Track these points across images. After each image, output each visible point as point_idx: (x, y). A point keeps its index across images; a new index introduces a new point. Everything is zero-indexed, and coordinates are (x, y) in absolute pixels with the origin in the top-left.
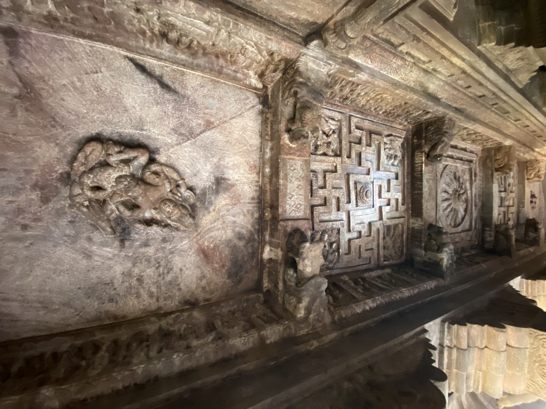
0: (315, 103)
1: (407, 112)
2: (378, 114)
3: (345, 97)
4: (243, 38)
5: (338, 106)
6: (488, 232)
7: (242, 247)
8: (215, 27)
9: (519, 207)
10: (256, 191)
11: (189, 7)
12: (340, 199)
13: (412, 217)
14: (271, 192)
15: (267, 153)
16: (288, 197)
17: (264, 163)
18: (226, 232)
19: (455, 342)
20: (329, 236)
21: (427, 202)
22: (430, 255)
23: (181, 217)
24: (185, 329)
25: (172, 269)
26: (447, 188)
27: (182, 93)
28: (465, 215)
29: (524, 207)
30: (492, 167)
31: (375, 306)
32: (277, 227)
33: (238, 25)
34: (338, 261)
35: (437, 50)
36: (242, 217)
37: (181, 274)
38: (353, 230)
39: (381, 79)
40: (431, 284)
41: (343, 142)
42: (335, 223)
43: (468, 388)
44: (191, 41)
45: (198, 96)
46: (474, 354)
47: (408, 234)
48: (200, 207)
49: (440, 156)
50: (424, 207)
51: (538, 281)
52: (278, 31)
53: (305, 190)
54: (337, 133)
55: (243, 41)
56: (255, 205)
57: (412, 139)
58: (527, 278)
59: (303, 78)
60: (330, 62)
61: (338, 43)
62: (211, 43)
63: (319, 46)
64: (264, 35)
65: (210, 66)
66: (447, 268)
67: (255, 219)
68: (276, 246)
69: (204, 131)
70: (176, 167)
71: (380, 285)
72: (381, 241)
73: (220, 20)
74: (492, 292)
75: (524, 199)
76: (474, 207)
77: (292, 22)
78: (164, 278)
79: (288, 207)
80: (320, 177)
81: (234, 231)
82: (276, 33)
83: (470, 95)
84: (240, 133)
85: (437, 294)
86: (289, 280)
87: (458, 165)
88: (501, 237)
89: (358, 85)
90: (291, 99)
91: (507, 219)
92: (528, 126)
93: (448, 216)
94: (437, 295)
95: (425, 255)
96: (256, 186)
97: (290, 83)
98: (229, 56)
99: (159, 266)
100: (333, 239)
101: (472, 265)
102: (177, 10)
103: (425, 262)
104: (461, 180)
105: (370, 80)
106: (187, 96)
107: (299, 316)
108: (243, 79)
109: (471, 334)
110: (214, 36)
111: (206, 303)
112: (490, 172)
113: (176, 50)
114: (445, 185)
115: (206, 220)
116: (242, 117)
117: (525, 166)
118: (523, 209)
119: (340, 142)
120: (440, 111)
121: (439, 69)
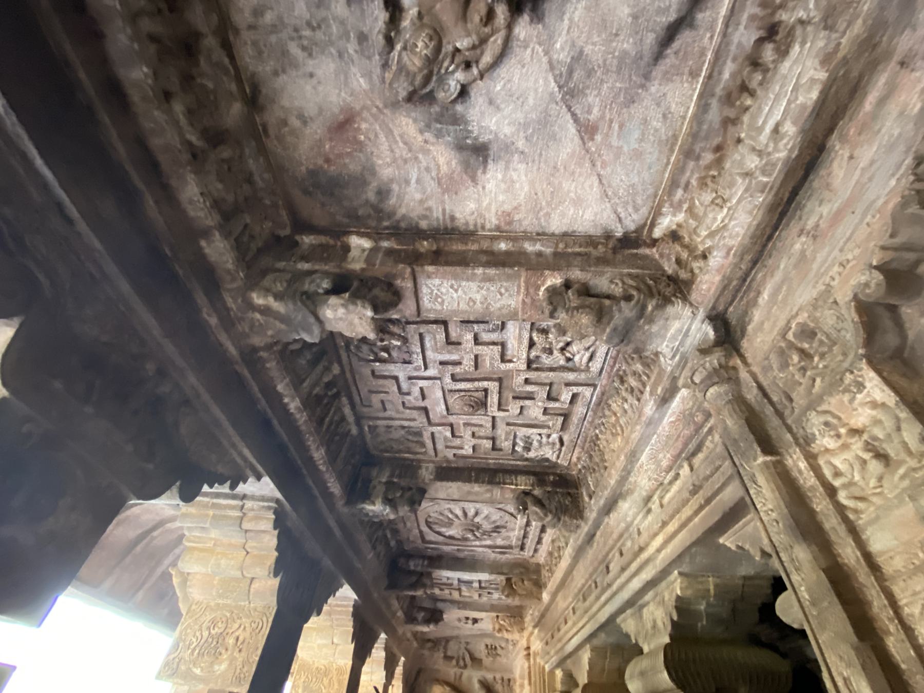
0: (608, 330)
1: (594, 470)
2: (596, 428)
3: (625, 378)
4: (739, 202)
5: (612, 367)
7: (364, 197)
8: (767, 145)
10: (467, 224)
11: (809, 90)
14: (464, 252)
15: (534, 245)
16: (453, 282)
17: (514, 239)
18: (389, 165)
19: (251, 514)
20: (399, 348)
21: (458, 488)
22: (381, 489)
23: (408, 73)
24: (203, 86)
25: (310, 55)
27: (654, 73)
28: (445, 536)
29: (459, 608)
31: (292, 411)
32: (402, 262)
33: (762, 192)
34: (361, 359)
35: (677, 516)
36: (418, 196)
37: (304, 75)
39: (642, 435)
40: (335, 488)
41: (551, 374)
42: (421, 357)
43: (189, 528)
44: (752, 94)
45: (646, 107)
46: (237, 539)
47: (412, 460)
48: (430, 114)
50: (450, 484)
52: (741, 269)
53: (466, 311)
54: (567, 365)
55: (734, 201)
56: (441, 222)
57: (554, 474)
58: (354, 606)
59: (653, 311)
60: (677, 358)
61: (701, 372)
62: (743, 135)
63: (704, 341)
64: (735, 242)
65: (703, 134)
67: (417, 223)
68: (369, 260)
69: (576, 120)
70: (506, 60)
71: (328, 419)
72: (397, 423)
73: (777, 155)
76: (456, 548)
77: (752, 295)
78: (292, 39)
79: (437, 281)
80: (494, 336)
81: (391, 181)
82: (736, 266)
83: (610, 556)
84: (572, 195)
86: (312, 282)
87: (516, 533)
88: (414, 579)
89: (639, 400)
90: (621, 290)
93: (441, 514)
95: (380, 482)
96: (475, 225)
97: (649, 287)
98: (716, 174)
99: (313, 29)
100: (395, 354)
101: (371, 541)
102: (809, 63)
103: (370, 481)
105: (644, 419)
106: (648, 84)
107: (254, 295)
108: (672, 201)
109: (263, 535)
110: (752, 143)
111: (260, 128)
112: (505, 571)
113: (740, 60)
114: (487, 514)
115: (407, 124)
116: (601, 197)
117: (516, 615)
119: (552, 369)
120: (591, 515)
121: (650, 518)
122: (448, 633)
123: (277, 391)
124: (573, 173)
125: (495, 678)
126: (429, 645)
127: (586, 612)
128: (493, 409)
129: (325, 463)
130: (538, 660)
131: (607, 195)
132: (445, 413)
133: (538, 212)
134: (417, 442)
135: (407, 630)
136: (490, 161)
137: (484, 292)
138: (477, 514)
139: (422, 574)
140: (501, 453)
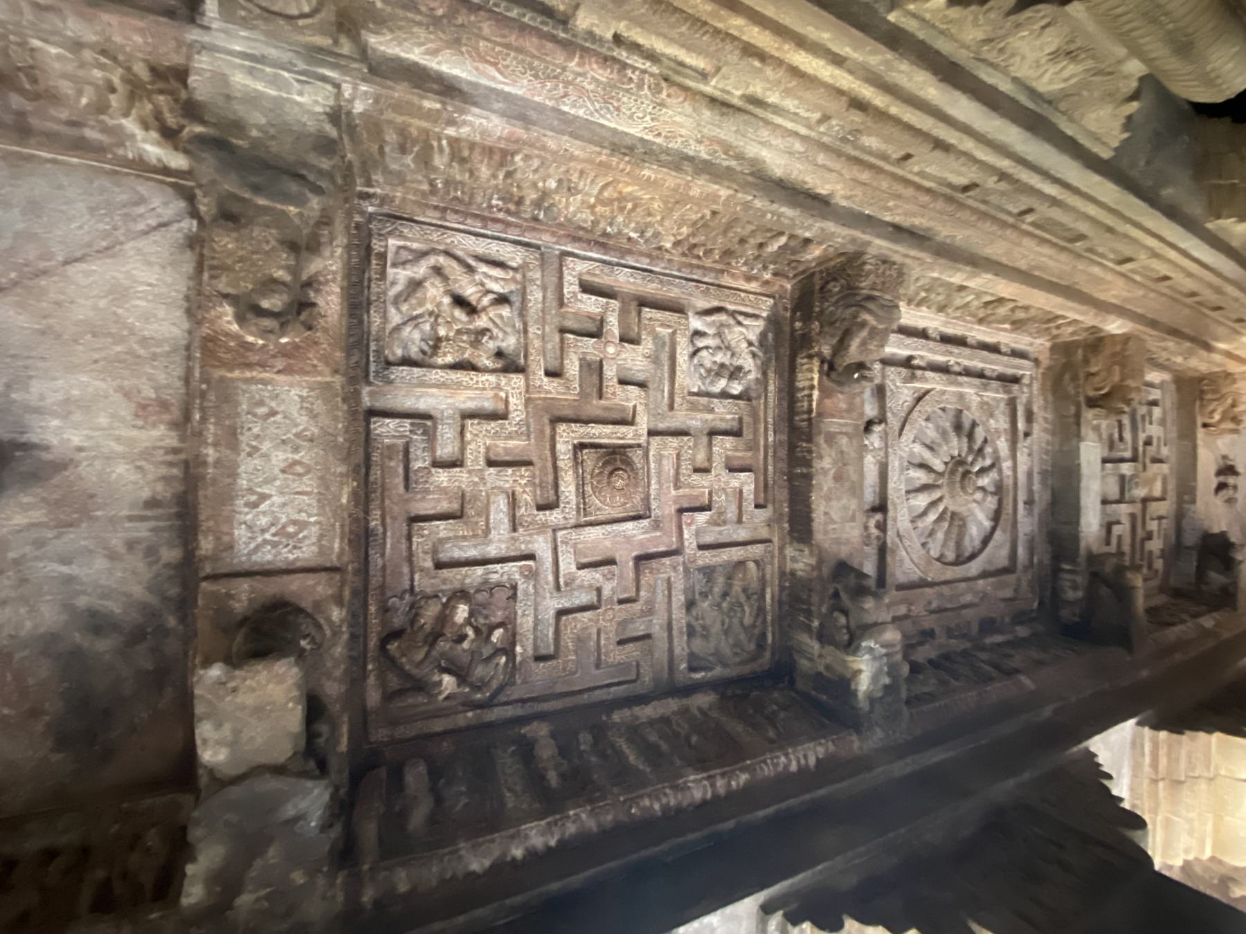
0: (261, 201)
5: (508, 224)
9: (1180, 502)
10: (166, 479)
12: (518, 497)
13: (791, 543)
16: (240, 502)
21: (828, 498)
26: (927, 456)
28: (994, 529)
29: (1193, 502)
30: (1077, 394)
36: (100, 563)
38: (567, 584)
42: (498, 567)
47: (782, 588)
49: (861, 366)
51: (1188, 733)
53: (322, 478)
57: (793, 320)
58: (1156, 727)
59: (203, 122)
74: (1011, 783)
75: (1195, 479)
79: (241, 533)
81: (68, 607)
91: (1140, 533)
92: (1166, 278)
94: (807, 797)
95: (820, 656)
104: (980, 434)
112: (1072, 409)
116: (113, 256)
118: (1192, 507)
120: (842, 236)
121: (773, 98)
124: (58, 304)
127: (1110, 230)
128: (625, 435)
131: (107, 249)
132: (645, 522)
133: (139, 357)
134: (730, 577)
136: (24, 438)
137: (266, 446)
139: (1094, 575)
140: (746, 419)
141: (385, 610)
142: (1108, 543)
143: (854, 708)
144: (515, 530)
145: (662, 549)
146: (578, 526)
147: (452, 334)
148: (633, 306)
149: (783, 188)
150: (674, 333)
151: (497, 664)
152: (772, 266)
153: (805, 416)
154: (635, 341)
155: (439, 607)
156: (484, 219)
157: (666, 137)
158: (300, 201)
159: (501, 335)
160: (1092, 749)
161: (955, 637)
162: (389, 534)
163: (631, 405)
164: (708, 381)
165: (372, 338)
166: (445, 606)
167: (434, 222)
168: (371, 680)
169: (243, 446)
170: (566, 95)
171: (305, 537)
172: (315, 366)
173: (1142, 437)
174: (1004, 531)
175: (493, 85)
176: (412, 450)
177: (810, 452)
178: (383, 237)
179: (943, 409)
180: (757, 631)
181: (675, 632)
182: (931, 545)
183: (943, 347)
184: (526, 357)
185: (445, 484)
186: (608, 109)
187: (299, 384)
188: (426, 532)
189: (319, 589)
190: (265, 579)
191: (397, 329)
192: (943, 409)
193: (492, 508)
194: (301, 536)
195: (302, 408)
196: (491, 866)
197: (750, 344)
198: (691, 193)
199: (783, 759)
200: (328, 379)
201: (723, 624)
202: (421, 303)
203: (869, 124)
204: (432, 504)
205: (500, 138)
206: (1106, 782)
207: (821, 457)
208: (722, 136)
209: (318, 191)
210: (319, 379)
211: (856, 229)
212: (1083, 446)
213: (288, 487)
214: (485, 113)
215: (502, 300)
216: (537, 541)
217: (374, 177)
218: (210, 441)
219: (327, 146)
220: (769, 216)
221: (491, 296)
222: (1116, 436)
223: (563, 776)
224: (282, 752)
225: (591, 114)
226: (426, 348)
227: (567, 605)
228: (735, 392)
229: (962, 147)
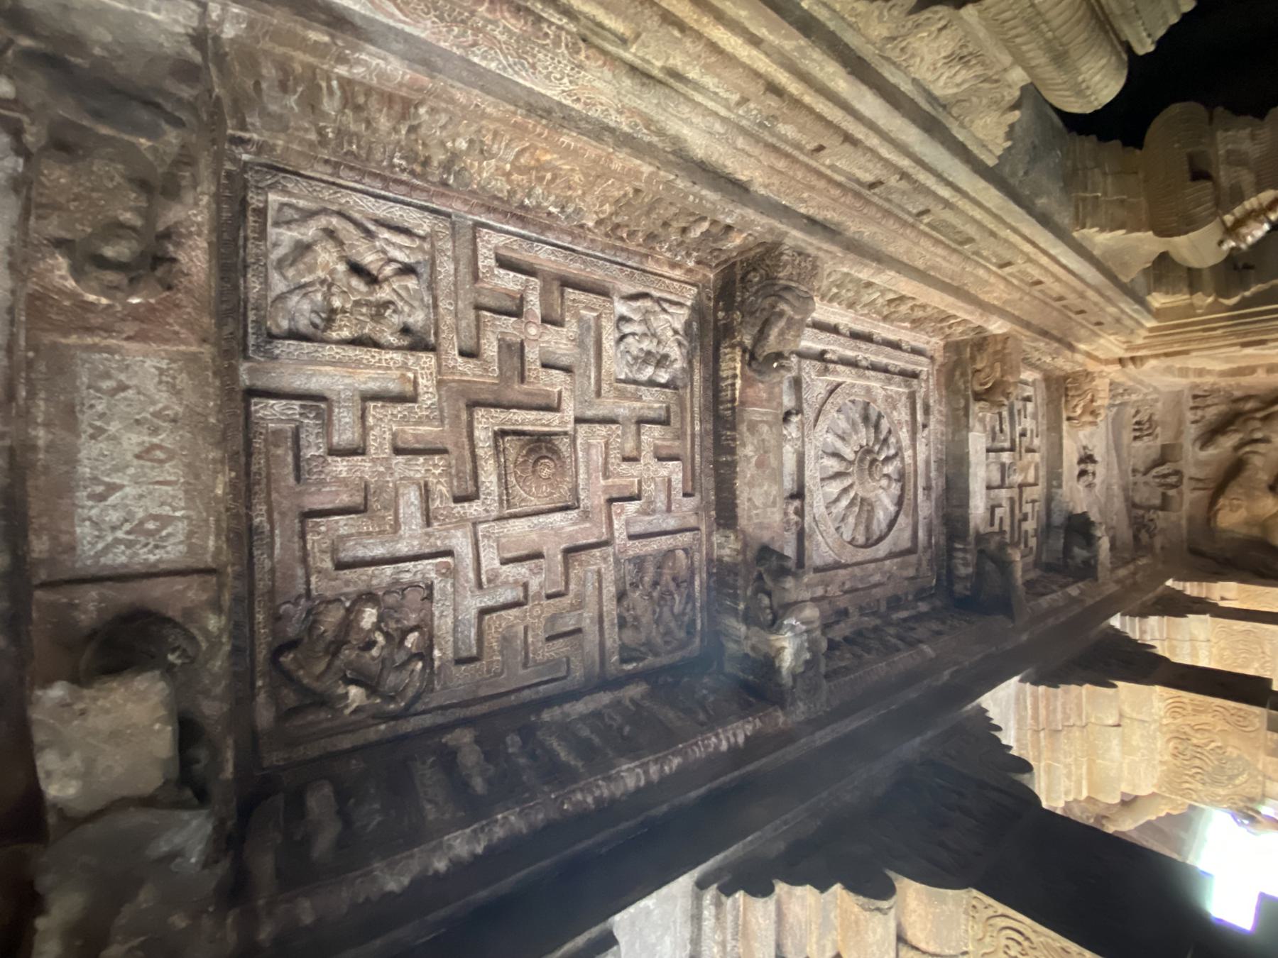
5: (414, 188)
6: (960, 555)
9: (1049, 486)
21: (751, 485)
26: (839, 444)
29: (1060, 486)
30: (966, 388)
38: (489, 581)
42: (410, 565)
47: (710, 574)
49: (779, 356)
53: (189, 465)
57: (716, 310)
66: (795, 676)
74: (918, 740)
75: (1061, 466)
79: (84, 531)
85: (738, 767)
87: (873, 384)
91: (1018, 515)
94: (736, 773)
95: (747, 638)
104: (885, 424)
109: (790, 919)
112: (962, 403)
117: (1061, 388)
118: (1060, 491)
121: (693, 74)
122: (1118, 504)
123: (406, 891)
125: (1193, 422)
126: (1144, 536)
127: (993, 234)
128: (550, 422)
129: (660, 761)
130: (1140, 341)
132: (573, 514)
134: (660, 567)
135: (1109, 580)
137: (113, 427)
138: (836, 455)
139: (981, 552)
140: (674, 408)
141: (276, 618)
142: (992, 524)
143: (780, 685)
144: (428, 524)
145: (592, 540)
146: (500, 519)
147: (348, 306)
148: (556, 284)
149: (704, 170)
150: (599, 317)
151: (413, 671)
152: (695, 254)
153: (729, 405)
154: (558, 323)
155: (342, 612)
156: (384, 179)
157: (586, 104)
158: (153, 133)
159: (406, 309)
160: (984, 706)
161: (867, 615)
162: (277, 532)
163: (556, 390)
164: (635, 368)
165: (250, 306)
166: (348, 610)
167: (325, 177)
168: (262, 698)
169: (84, 426)
170: (475, 44)
171: (169, 535)
172: (177, 333)
173: (1018, 429)
174: (907, 516)
175: (391, 23)
176: (303, 436)
177: (734, 440)
178: (263, 190)
179: (853, 402)
180: (686, 619)
181: (606, 625)
182: (843, 529)
183: (852, 342)
184: (436, 334)
185: (344, 474)
186: (522, 65)
187: (156, 354)
188: (323, 529)
189: (190, 594)
190: (118, 585)
191: (281, 297)
192: (853, 402)
193: (402, 502)
194: (164, 533)
195: (160, 382)
196: (412, 882)
197: (676, 332)
198: (613, 167)
199: (714, 739)
200: (194, 349)
201: (654, 612)
202: (311, 269)
203: (785, 110)
204: (329, 498)
205: (401, 85)
206: (997, 734)
207: (744, 445)
208: (642, 108)
209: (177, 123)
210: (182, 348)
211: (773, 218)
212: (971, 435)
213: (145, 475)
214: (383, 53)
215: (407, 270)
216: (455, 536)
217: (248, 120)
218: (39, 420)
219: (187, 71)
220: (691, 198)
221: (394, 266)
222: (998, 428)
223: (489, 782)
224: (151, 780)
225: (504, 69)
226: (318, 321)
227: (490, 603)
228: (663, 381)
229: (868, 143)
